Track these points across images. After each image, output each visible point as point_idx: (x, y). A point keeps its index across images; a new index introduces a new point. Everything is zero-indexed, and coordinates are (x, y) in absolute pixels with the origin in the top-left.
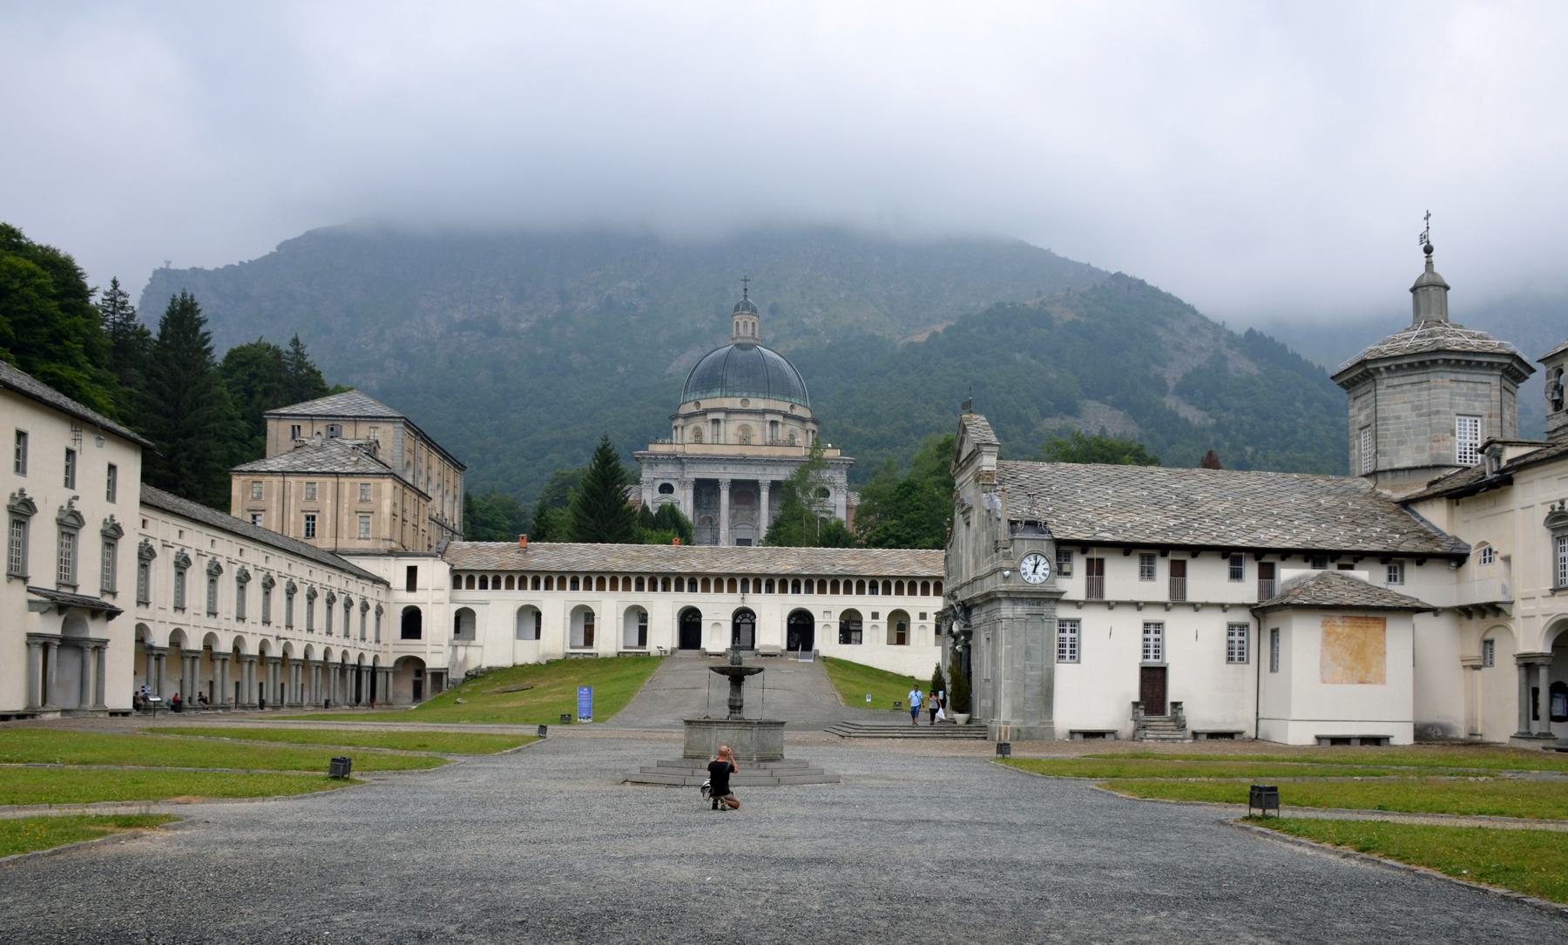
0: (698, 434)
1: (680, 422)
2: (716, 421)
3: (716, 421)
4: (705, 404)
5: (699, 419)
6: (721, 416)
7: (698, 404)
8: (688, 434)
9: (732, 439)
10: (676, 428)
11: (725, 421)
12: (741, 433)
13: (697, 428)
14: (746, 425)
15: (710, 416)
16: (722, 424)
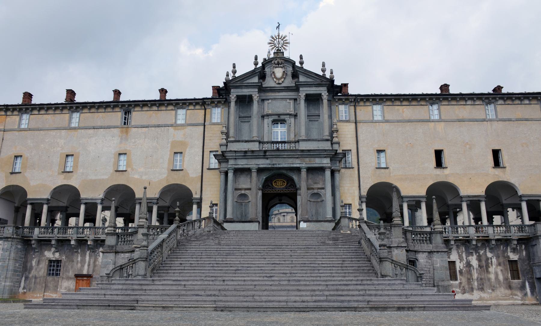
0: (279, 220)
1: (273, 216)
2: (284, 216)
3: (284, 216)
4: (281, 211)
5: (279, 215)
6: (285, 214)
7: (279, 211)
8: (276, 219)
9: (289, 221)
10: (273, 218)
11: (287, 216)
12: (291, 219)
13: (278, 218)
14: (292, 216)
15: (282, 214)
16: (286, 216)
